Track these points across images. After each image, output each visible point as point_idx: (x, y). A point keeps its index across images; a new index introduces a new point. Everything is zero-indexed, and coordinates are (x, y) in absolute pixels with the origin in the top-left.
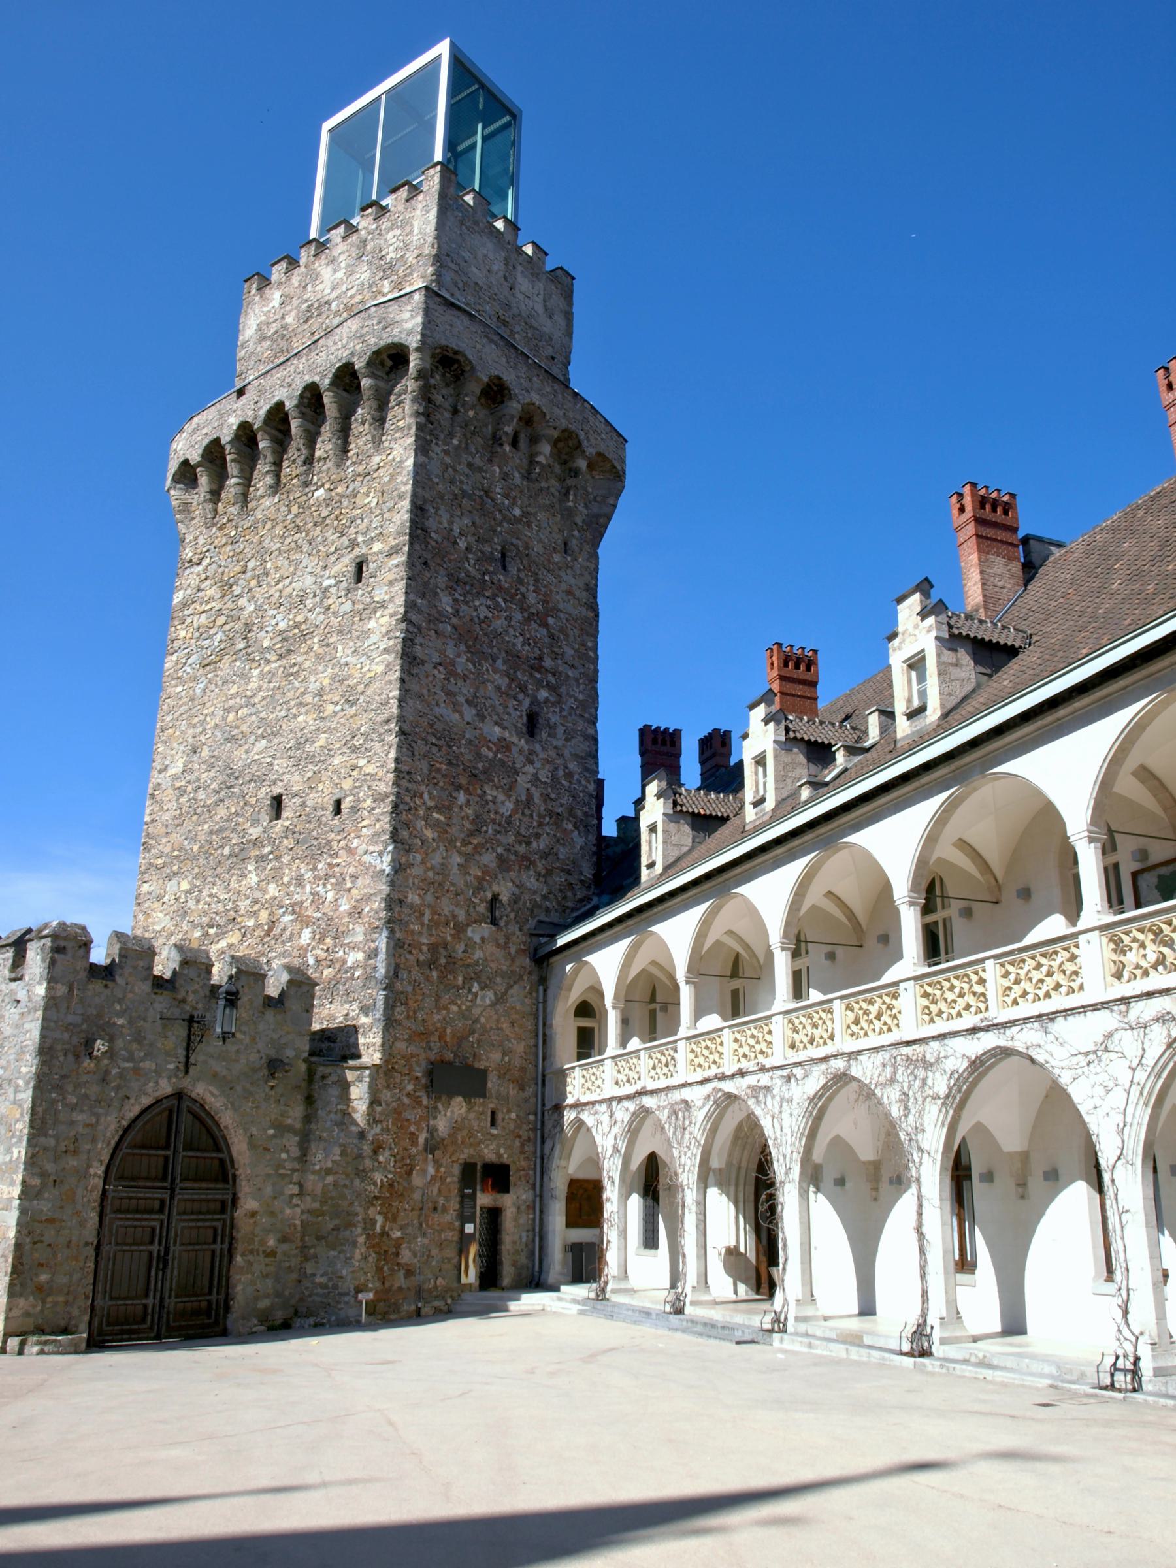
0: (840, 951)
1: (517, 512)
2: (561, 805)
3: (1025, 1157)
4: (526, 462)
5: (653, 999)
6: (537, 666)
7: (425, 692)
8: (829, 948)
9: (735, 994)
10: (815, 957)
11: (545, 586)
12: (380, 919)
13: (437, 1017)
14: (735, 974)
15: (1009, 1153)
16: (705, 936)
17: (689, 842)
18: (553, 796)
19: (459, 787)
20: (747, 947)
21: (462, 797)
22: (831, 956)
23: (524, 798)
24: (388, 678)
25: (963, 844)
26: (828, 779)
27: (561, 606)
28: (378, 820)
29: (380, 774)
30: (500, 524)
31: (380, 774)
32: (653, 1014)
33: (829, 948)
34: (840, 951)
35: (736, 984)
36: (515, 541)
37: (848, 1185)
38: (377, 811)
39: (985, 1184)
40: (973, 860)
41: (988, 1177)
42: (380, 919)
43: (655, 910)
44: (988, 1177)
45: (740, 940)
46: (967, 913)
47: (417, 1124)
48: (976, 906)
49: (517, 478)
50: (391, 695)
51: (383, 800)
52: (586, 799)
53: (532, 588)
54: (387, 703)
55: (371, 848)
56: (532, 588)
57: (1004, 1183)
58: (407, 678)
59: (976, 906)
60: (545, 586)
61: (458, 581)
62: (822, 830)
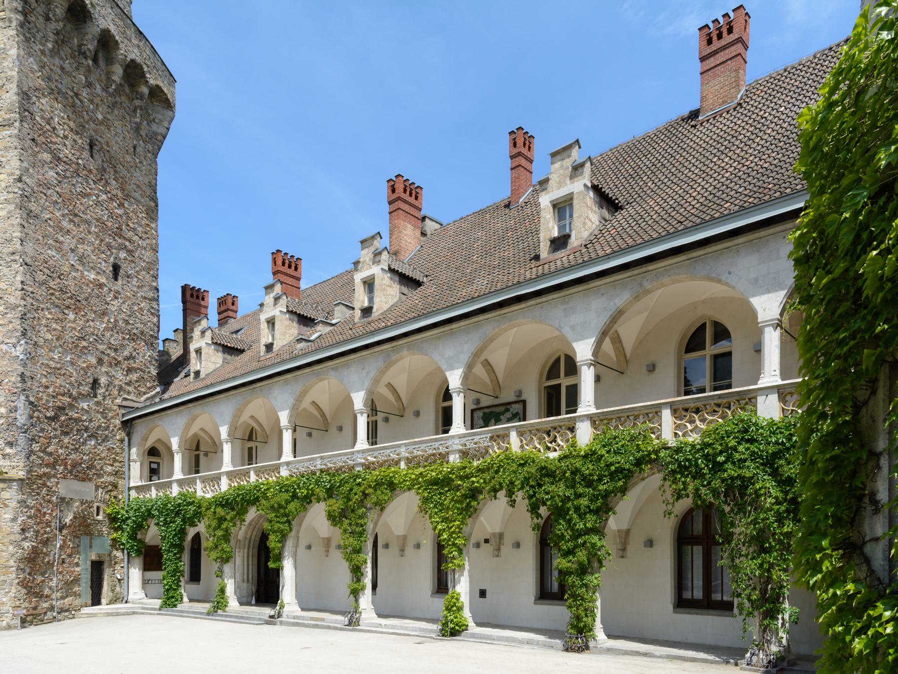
0: (314, 433)
1: (100, 117)
2: (137, 329)
3: (405, 538)
4: (104, 78)
5: (198, 448)
6: (119, 233)
7: (40, 238)
8: (308, 430)
9: (250, 449)
10: (302, 433)
11: (122, 178)
12: (17, 388)
13: (60, 451)
14: (250, 439)
15: (398, 536)
16: (239, 417)
17: (220, 361)
18: (131, 322)
19: (68, 307)
20: (261, 425)
21: (72, 316)
22: (310, 435)
23: (112, 320)
24: (10, 221)
25: (390, 386)
26: (312, 338)
27: (133, 194)
28: (11, 322)
29: (9, 290)
30: (87, 122)
31: (9, 290)
32: (197, 458)
33: (308, 430)
34: (314, 433)
35: (250, 444)
36: (99, 139)
37: (313, 549)
38: (9, 315)
39: (384, 550)
40: (393, 394)
41: (386, 546)
42: (17, 388)
43: (207, 400)
44: (386, 546)
45: (257, 421)
46: (386, 420)
47: (51, 514)
48: (391, 417)
49: (99, 89)
50: (14, 235)
51: (14, 309)
52: (152, 326)
53: (113, 177)
54: (11, 240)
55: (7, 341)
56: (113, 177)
57: (394, 548)
58: (26, 225)
59: (391, 417)
60: (122, 178)
61: (59, 159)
62: (315, 368)
